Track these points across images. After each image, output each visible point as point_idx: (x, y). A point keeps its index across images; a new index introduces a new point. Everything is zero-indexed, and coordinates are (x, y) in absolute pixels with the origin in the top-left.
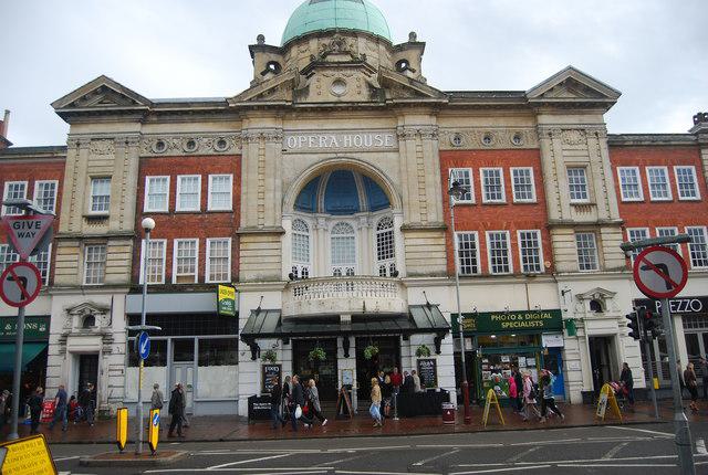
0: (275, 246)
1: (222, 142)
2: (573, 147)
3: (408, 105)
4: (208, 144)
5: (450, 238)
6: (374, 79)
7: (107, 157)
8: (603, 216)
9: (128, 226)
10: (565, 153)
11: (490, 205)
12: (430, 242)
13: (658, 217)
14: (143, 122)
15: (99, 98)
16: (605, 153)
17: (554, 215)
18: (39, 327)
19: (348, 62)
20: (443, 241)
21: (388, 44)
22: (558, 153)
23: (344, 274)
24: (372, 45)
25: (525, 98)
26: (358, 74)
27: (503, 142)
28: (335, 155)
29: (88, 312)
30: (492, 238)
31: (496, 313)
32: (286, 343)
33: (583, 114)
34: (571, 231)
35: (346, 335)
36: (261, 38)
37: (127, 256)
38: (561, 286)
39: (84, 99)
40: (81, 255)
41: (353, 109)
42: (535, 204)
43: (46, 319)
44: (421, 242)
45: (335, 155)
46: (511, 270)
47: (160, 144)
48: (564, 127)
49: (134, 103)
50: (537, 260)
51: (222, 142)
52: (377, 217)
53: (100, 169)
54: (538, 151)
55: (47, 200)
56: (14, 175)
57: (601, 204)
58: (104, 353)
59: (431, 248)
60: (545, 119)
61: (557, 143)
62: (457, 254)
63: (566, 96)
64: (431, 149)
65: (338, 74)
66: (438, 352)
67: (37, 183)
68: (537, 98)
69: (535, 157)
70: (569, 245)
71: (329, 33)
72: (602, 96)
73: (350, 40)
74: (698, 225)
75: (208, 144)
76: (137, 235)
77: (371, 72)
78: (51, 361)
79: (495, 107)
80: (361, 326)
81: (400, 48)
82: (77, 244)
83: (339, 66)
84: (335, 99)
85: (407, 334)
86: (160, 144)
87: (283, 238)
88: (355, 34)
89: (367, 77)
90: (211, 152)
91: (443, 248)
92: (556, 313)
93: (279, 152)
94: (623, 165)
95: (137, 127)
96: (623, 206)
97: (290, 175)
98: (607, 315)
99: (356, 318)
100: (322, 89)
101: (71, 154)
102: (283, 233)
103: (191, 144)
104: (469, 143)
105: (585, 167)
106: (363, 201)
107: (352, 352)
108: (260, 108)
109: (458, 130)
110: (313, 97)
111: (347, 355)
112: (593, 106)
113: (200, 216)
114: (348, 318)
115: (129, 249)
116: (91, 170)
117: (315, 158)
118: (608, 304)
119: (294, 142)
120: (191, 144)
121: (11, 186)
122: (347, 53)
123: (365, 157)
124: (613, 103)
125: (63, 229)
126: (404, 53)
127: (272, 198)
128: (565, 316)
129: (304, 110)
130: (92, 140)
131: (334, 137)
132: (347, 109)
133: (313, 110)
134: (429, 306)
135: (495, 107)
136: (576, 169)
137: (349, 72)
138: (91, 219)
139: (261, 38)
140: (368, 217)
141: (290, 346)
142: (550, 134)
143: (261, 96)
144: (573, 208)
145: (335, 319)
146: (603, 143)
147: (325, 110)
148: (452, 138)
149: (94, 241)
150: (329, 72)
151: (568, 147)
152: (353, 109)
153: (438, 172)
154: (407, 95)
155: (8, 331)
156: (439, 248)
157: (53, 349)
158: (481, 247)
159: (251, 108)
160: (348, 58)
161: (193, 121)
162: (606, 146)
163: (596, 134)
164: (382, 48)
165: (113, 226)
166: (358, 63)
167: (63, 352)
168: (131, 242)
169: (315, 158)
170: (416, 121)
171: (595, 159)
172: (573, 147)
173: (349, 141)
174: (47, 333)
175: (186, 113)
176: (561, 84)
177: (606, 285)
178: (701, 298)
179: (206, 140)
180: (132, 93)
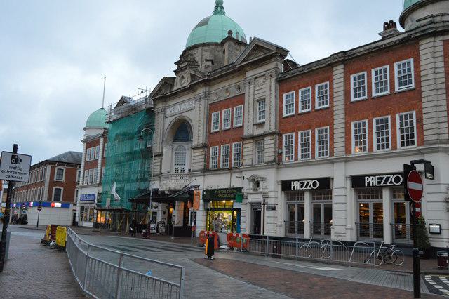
0: (159, 160)
2: (261, 87)
11: (357, 102)
13: (301, 124)
17: (245, 133)
21: (216, 44)
22: (251, 94)
24: (206, 48)
27: (236, 92)
30: (356, 127)
31: (217, 190)
33: (264, 65)
34: (251, 141)
38: (243, 174)
41: (183, 91)
57: (267, 123)
60: (250, 74)
61: (252, 86)
62: (211, 159)
63: (260, 55)
64: (203, 105)
68: (242, 62)
69: (240, 99)
73: (195, 51)
74: (323, 126)
79: (226, 75)
81: (223, 43)
88: (196, 47)
92: (240, 189)
94: (303, 87)
98: (260, 190)
100: (177, 87)
105: (265, 99)
110: (175, 88)
117: (173, 118)
118: (261, 183)
119: (169, 112)
128: (243, 191)
135: (230, 73)
136: (261, 101)
144: (255, 127)
147: (176, 94)
152: (183, 91)
170: (201, 91)
171: (268, 93)
172: (261, 87)
177: (260, 173)
178: (318, 179)
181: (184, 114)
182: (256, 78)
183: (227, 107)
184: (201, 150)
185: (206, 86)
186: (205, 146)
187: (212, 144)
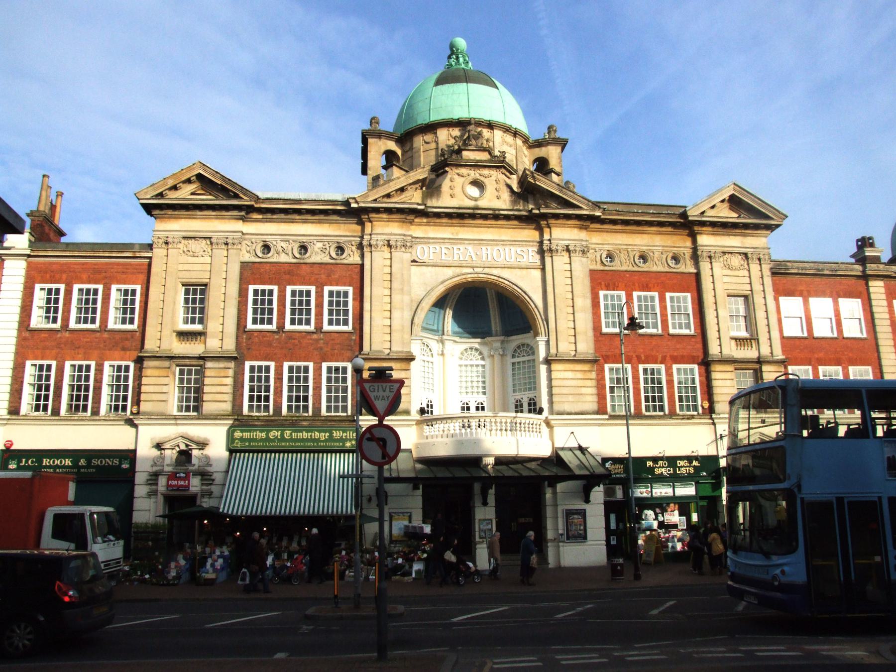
1: (340, 249)
3: (556, 216)
4: (323, 250)
5: (601, 371)
6: (514, 183)
7: (201, 260)
8: (765, 351)
9: (230, 345)
10: (726, 279)
12: (579, 375)
14: (243, 219)
15: (192, 187)
16: (768, 280)
17: (714, 350)
18: (121, 464)
19: (485, 161)
20: (593, 375)
23: (473, 409)
25: (684, 215)
26: (495, 174)
28: (471, 270)
29: (183, 447)
32: (416, 488)
33: (745, 235)
34: (730, 368)
35: (487, 481)
36: (374, 120)
37: (230, 381)
39: (175, 188)
40: (171, 376)
41: (495, 216)
42: (693, 336)
43: (130, 454)
44: (570, 375)
45: (471, 270)
46: (667, 412)
47: (267, 248)
48: (726, 250)
49: (236, 196)
50: (695, 399)
51: (340, 249)
52: (517, 340)
53: (194, 275)
54: (698, 276)
55: (127, 310)
56: (85, 276)
58: (203, 496)
59: (581, 383)
60: (706, 240)
65: (474, 174)
66: (587, 501)
67: (114, 287)
70: (728, 383)
71: (462, 124)
72: (767, 217)
73: (486, 133)
75: (323, 250)
76: (237, 359)
77: (511, 173)
78: (138, 504)
80: (506, 472)
82: (166, 363)
83: (477, 165)
84: (471, 204)
85: (553, 481)
86: (267, 248)
87: (412, 363)
88: (490, 126)
89: (507, 180)
90: (327, 259)
91: (594, 383)
93: (407, 263)
95: (239, 226)
96: (784, 340)
97: (418, 291)
99: (500, 461)
101: (158, 253)
102: (412, 359)
103: (304, 248)
104: (622, 265)
106: (495, 323)
107: (491, 499)
108: (389, 211)
109: (607, 247)
111: (485, 503)
112: (757, 227)
113: (315, 336)
114: (490, 461)
115: (231, 373)
116: (181, 275)
117: (449, 272)
120: (304, 248)
121: (81, 290)
122: (484, 150)
123: (506, 274)
124: (778, 226)
125: (150, 344)
126: (543, 149)
127: (401, 317)
129: (438, 215)
130: (184, 238)
131: (470, 248)
132: (485, 217)
133: (449, 216)
134: (581, 448)
137: (486, 172)
138: (183, 335)
139: (374, 120)
140: (503, 342)
141: (420, 492)
142: (710, 257)
143: (388, 196)
144: (733, 342)
145: (475, 461)
146: (766, 268)
148: (604, 256)
149: (187, 362)
150: (464, 171)
151: (729, 272)
152: (495, 216)
153: (589, 295)
154: (554, 205)
155: (83, 467)
156: (589, 383)
157: (140, 490)
158: (633, 383)
159: (377, 210)
160: (484, 156)
161: (305, 221)
162: (769, 274)
163: (759, 259)
164: (519, 142)
165: (213, 344)
166: (500, 164)
167: (152, 494)
168: (232, 364)
169: (449, 272)
173: (489, 254)
174: (132, 470)
175: (298, 212)
176: (723, 201)
179: (320, 245)
180: (234, 184)
181: (495, 272)
182: (724, 253)
183: (646, 288)
184: (586, 367)
185: (581, 228)
186: (595, 362)
187: (607, 359)
